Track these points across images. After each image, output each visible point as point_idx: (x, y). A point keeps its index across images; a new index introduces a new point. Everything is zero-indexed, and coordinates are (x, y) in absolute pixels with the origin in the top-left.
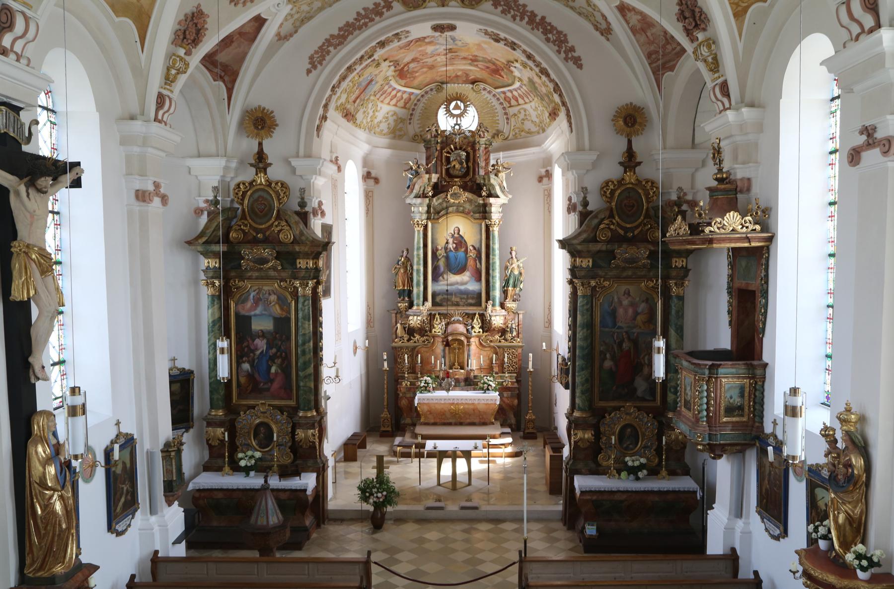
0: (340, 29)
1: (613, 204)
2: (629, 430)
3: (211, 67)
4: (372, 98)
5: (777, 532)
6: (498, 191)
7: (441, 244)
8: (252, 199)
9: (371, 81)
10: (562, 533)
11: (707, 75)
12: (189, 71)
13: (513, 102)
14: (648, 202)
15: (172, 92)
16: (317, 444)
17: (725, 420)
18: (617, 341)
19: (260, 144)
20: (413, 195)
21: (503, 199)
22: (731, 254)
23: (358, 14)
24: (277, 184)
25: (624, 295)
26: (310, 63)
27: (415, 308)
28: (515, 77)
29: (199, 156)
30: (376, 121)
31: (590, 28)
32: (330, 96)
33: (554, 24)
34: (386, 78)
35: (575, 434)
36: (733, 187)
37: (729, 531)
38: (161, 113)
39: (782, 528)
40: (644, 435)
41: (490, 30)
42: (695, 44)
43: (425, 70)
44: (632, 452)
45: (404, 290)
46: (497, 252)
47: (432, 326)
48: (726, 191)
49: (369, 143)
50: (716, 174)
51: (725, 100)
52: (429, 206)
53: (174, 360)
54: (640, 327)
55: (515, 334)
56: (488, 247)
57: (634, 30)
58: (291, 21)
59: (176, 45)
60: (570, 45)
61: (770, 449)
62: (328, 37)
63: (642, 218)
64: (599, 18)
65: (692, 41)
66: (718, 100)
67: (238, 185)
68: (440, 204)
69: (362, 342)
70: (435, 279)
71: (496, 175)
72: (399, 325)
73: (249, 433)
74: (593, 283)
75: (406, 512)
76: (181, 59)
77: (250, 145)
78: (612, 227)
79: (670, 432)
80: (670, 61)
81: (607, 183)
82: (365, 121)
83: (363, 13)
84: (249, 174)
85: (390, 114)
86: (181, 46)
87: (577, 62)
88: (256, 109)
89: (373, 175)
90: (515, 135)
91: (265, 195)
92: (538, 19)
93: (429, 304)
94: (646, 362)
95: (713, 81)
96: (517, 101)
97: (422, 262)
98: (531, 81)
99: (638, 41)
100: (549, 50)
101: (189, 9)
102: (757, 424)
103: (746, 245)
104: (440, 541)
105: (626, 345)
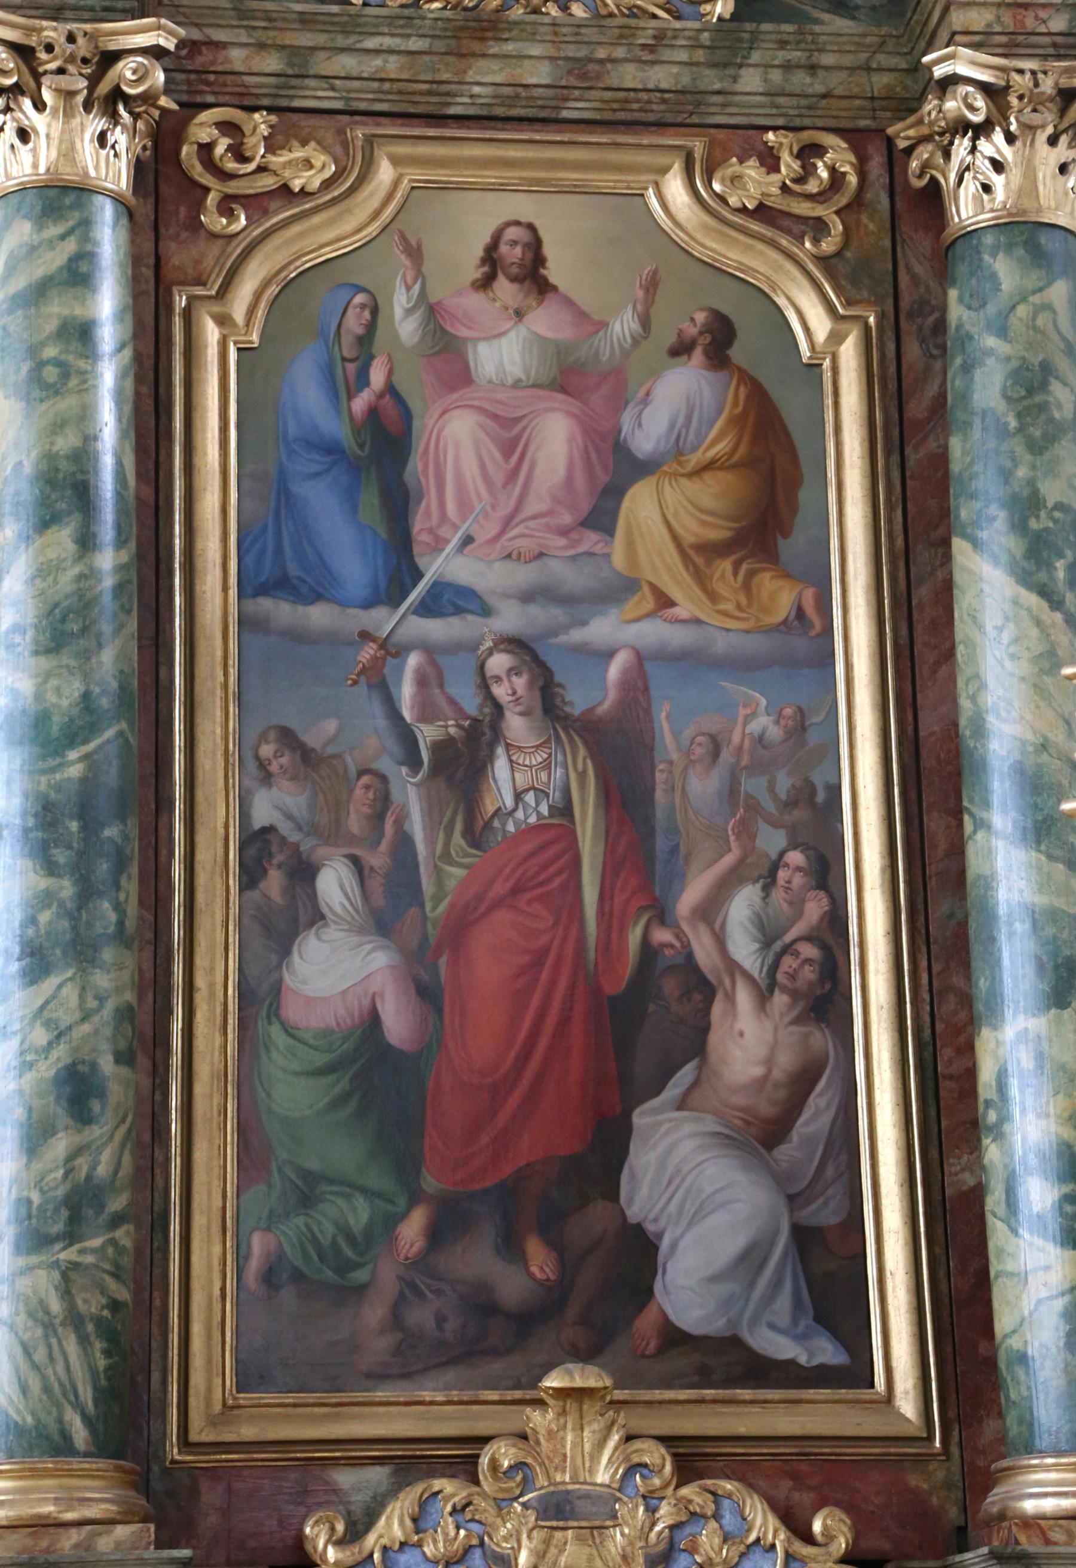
18: (427, 734)
25: (485, 283)
54: (664, 602)
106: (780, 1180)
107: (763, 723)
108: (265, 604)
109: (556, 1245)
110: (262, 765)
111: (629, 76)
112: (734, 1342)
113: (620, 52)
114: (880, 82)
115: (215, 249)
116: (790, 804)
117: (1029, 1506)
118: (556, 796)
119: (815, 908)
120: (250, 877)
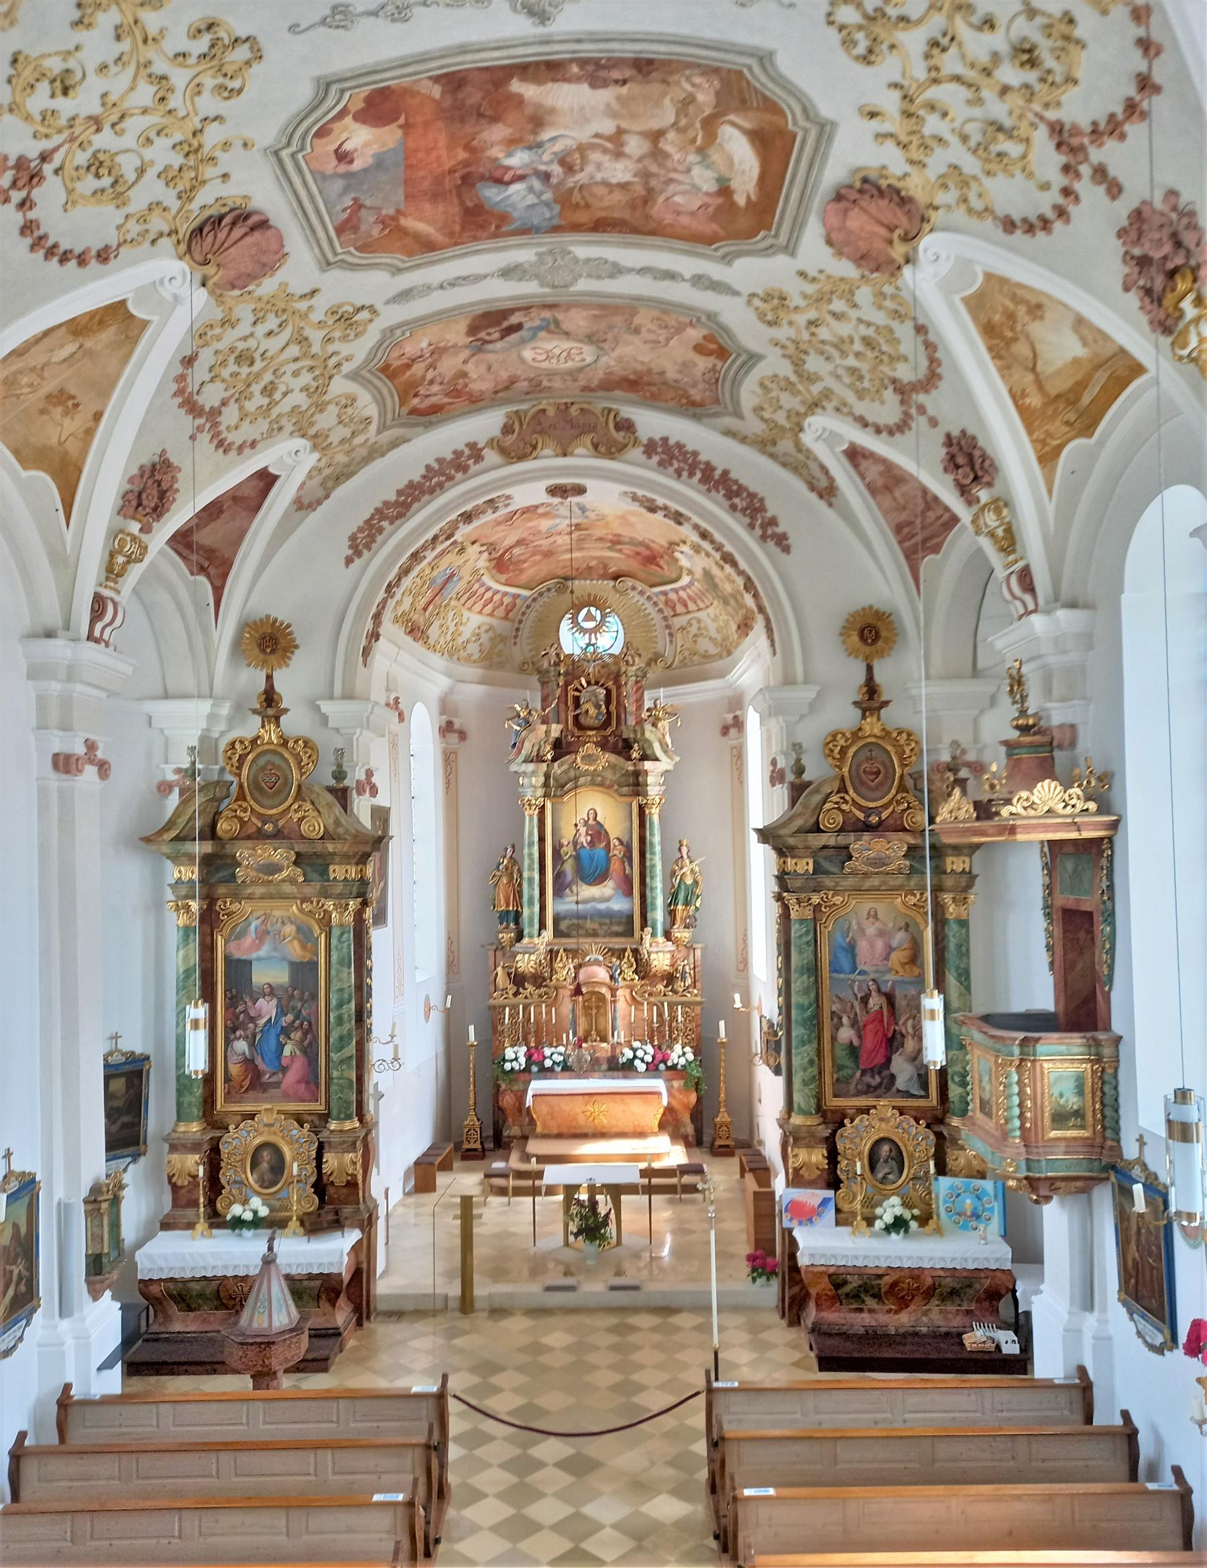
0: (400, 493)
1: (846, 770)
2: (886, 1148)
3: (186, 552)
4: (453, 603)
5: (1159, 1339)
6: (658, 752)
7: (567, 835)
8: (254, 768)
9: (452, 576)
10: (781, 1334)
11: (995, 558)
12: (148, 559)
13: (680, 609)
14: (903, 766)
15: (118, 592)
16: (360, 1178)
17: (1054, 1134)
19: (269, 678)
20: (521, 758)
21: (665, 764)
22: (1046, 849)
23: (428, 467)
24: (296, 742)
26: (351, 547)
27: (526, 940)
28: (681, 568)
29: (166, 696)
30: (460, 640)
31: (802, 487)
32: (384, 601)
33: (744, 481)
34: (476, 572)
35: (795, 1156)
36: (1046, 739)
37: (1072, 1335)
38: (99, 627)
39: (1167, 1332)
40: (911, 1156)
41: (640, 493)
42: (975, 508)
43: (538, 558)
45: (508, 912)
46: (658, 848)
47: (553, 971)
48: (1035, 747)
49: (448, 674)
50: (1017, 719)
51: (1028, 598)
52: (547, 776)
53: (116, 1037)
55: (689, 981)
56: (642, 840)
57: (873, 490)
58: (318, 479)
59: (125, 517)
60: (769, 514)
61: (1138, 1189)
62: (380, 505)
63: (893, 791)
64: (816, 472)
65: (970, 503)
66: (1014, 597)
67: (233, 744)
68: (565, 772)
69: (436, 999)
70: (559, 892)
71: (654, 725)
72: (499, 970)
73: (242, 1161)
74: (816, 899)
75: (511, 1296)
76: (134, 539)
77: (253, 679)
78: (844, 807)
81: (834, 736)
82: (442, 641)
83: (436, 466)
84: (252, 727)
85: (484, 628)
86: (134, 518)
87: (782, 542)
88: (261, 620)
89: (457, 726)
90: (683, 664)
91: (277, 761)
92: (717, 474)
93: (548, 934)
94: (910, 1030)
95: (1007, 566)
96: (686, 606)
97: (536, 866)
98: (707, 574)
99: (880, 506)
100: (736, 525)
101: (146, 459)
102: (1109, 1143)
103: (1074, 835)
104: (568, 1349)
105: (875, 1002)
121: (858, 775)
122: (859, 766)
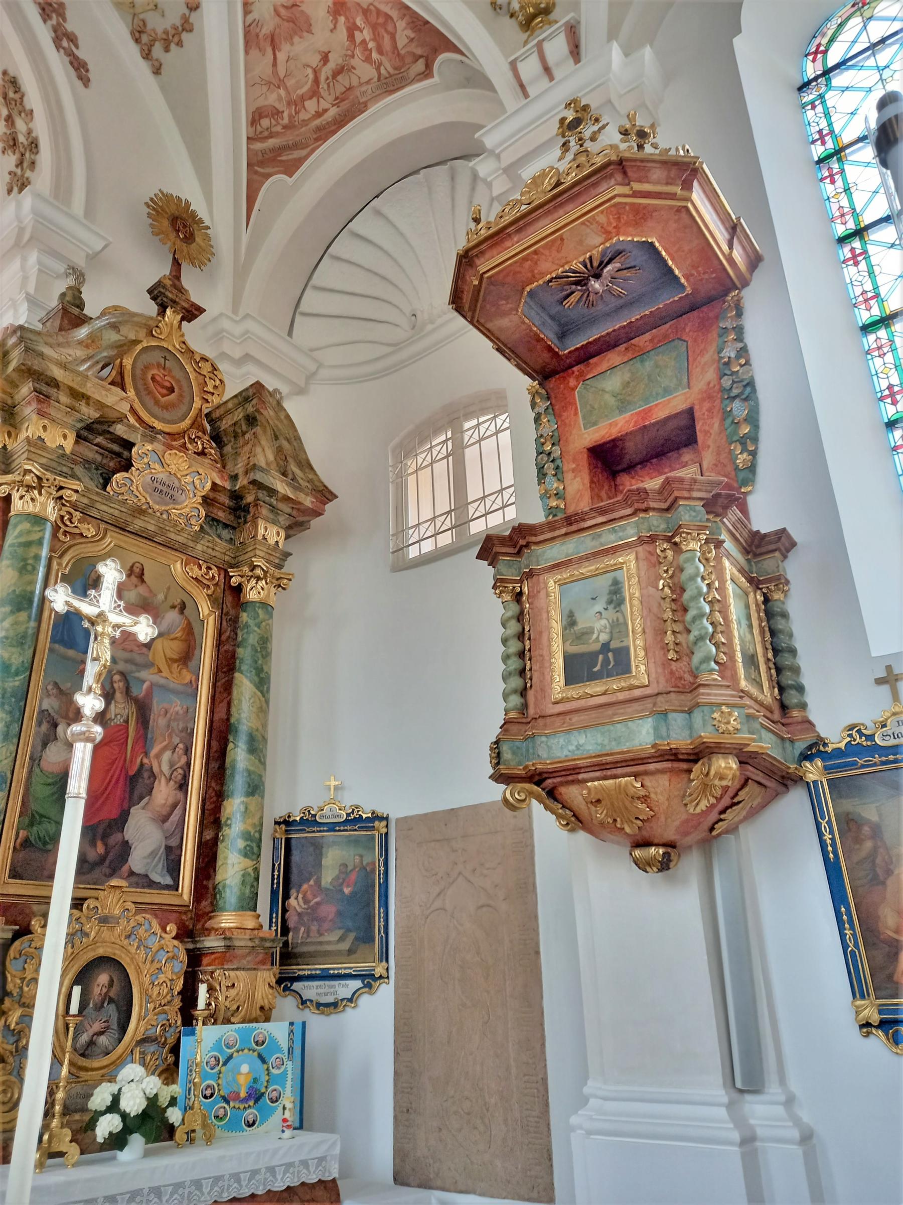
44: (105, 1061)
54: (160, 671)
57: (251, 38)
63: (188, 422)
79: (232, 973)
80: (296, 146)
94: (165, 768)
99: (247, 70)
106: (164, 831)
107: (178, 708)
108: (57, 646)
109: (106, 845)
110: (48, 691)
111: (172, 536)
112: (147, 876)
113: (172, 529)
114: (227, 558)
115: (60, 544)
116: (182, 731)
117: (223, 925)
118: (125, 717)
119: (184, 760)
120: (39, 724)
121: (144, 379)
122: (147, 368)
